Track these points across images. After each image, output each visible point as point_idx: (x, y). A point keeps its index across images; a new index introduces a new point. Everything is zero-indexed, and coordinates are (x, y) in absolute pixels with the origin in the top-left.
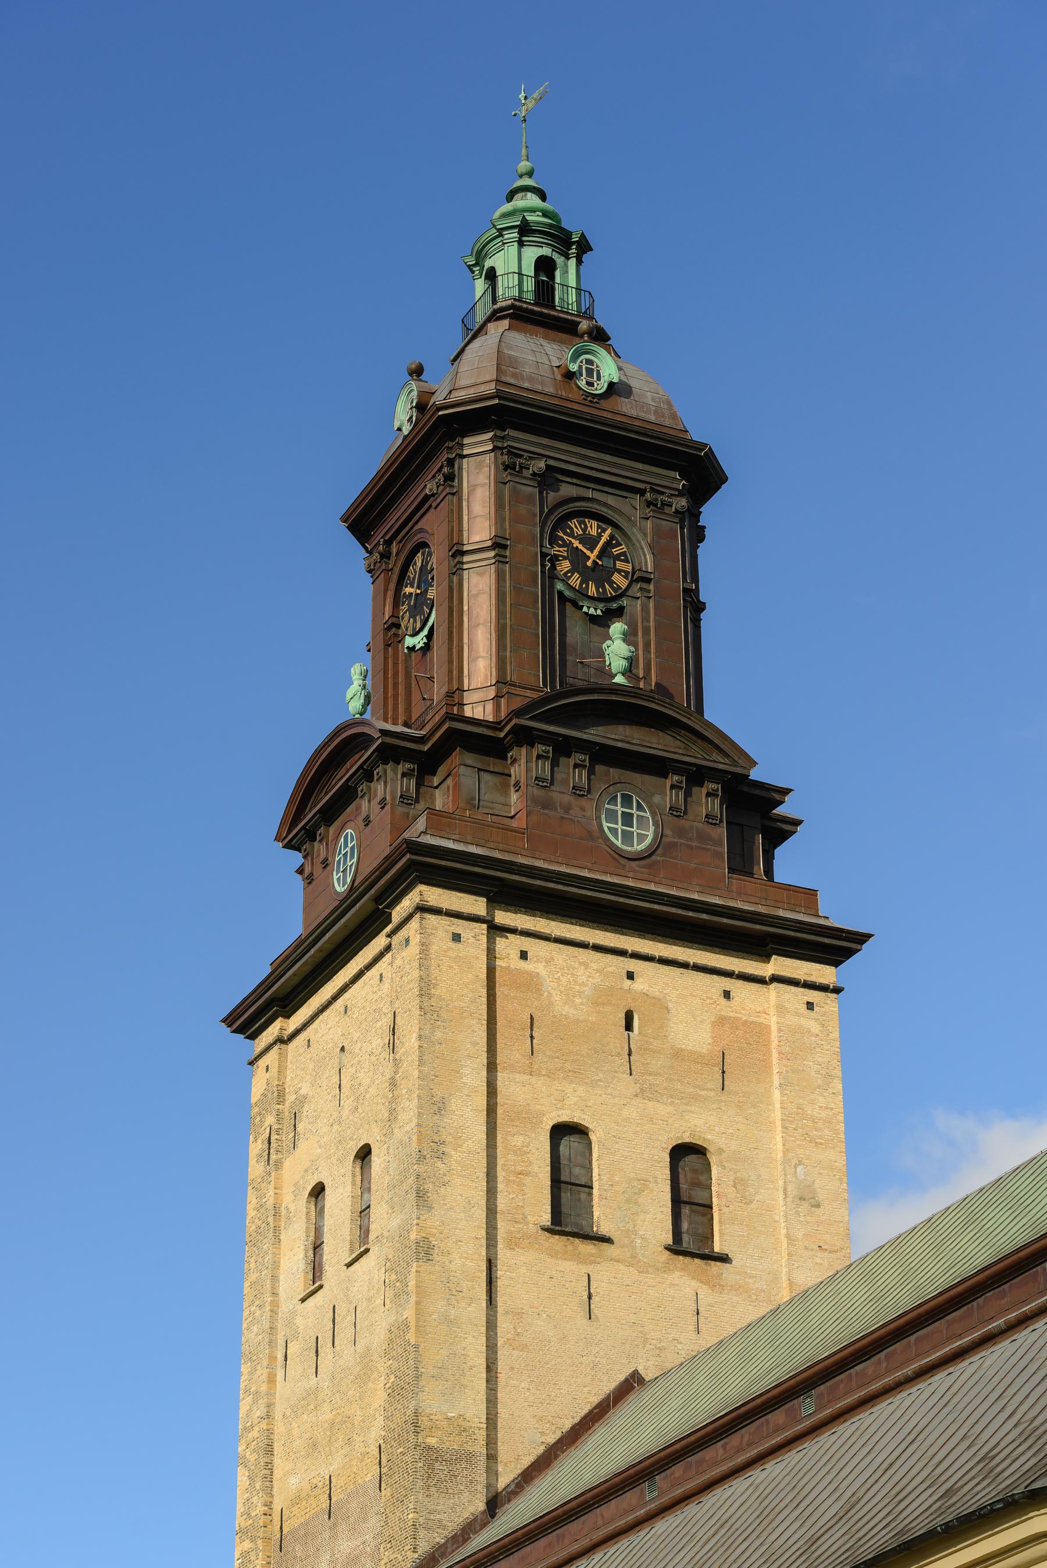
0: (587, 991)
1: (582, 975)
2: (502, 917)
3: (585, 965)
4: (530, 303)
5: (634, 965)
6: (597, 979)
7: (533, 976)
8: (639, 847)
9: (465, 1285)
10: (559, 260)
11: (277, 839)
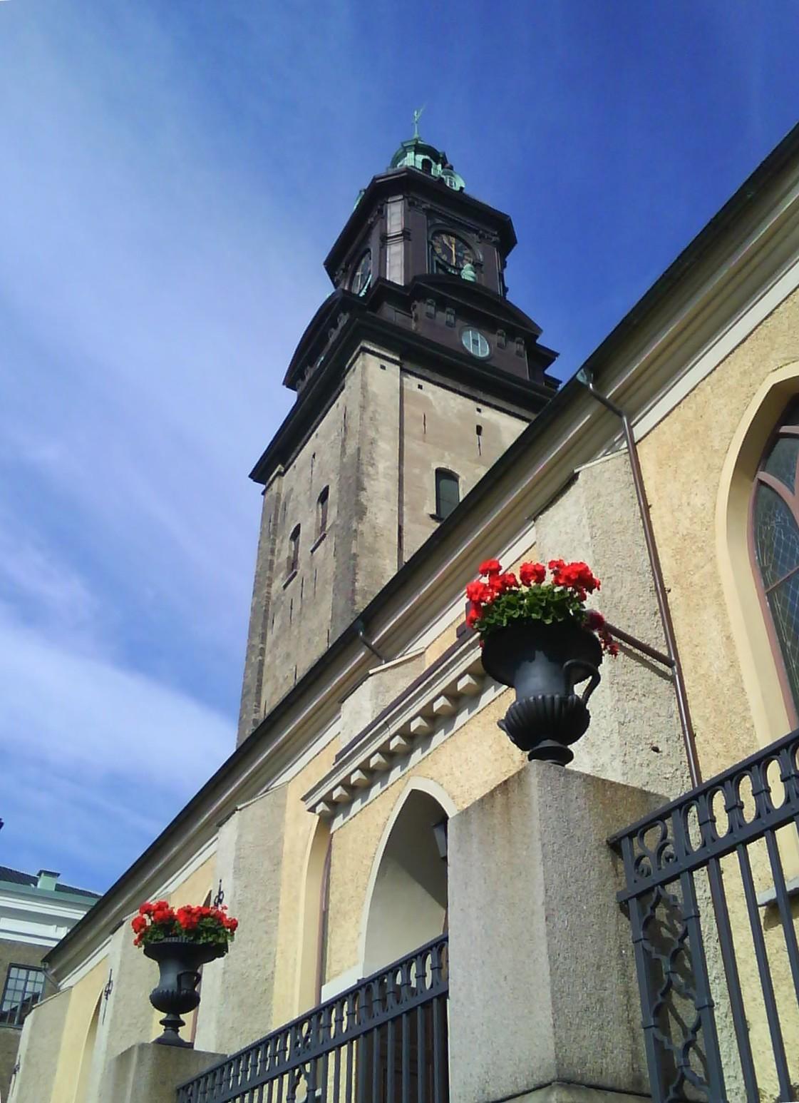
0: (455, 411)
1: (452, 403)
2: (407, 366)
3: (455, 400)
4: (419, 169)
5: (480, 406)
7: (426, 398)
8: (480, 355)
9: (386, 533)
10: (434, 163)
11: (284, 384)
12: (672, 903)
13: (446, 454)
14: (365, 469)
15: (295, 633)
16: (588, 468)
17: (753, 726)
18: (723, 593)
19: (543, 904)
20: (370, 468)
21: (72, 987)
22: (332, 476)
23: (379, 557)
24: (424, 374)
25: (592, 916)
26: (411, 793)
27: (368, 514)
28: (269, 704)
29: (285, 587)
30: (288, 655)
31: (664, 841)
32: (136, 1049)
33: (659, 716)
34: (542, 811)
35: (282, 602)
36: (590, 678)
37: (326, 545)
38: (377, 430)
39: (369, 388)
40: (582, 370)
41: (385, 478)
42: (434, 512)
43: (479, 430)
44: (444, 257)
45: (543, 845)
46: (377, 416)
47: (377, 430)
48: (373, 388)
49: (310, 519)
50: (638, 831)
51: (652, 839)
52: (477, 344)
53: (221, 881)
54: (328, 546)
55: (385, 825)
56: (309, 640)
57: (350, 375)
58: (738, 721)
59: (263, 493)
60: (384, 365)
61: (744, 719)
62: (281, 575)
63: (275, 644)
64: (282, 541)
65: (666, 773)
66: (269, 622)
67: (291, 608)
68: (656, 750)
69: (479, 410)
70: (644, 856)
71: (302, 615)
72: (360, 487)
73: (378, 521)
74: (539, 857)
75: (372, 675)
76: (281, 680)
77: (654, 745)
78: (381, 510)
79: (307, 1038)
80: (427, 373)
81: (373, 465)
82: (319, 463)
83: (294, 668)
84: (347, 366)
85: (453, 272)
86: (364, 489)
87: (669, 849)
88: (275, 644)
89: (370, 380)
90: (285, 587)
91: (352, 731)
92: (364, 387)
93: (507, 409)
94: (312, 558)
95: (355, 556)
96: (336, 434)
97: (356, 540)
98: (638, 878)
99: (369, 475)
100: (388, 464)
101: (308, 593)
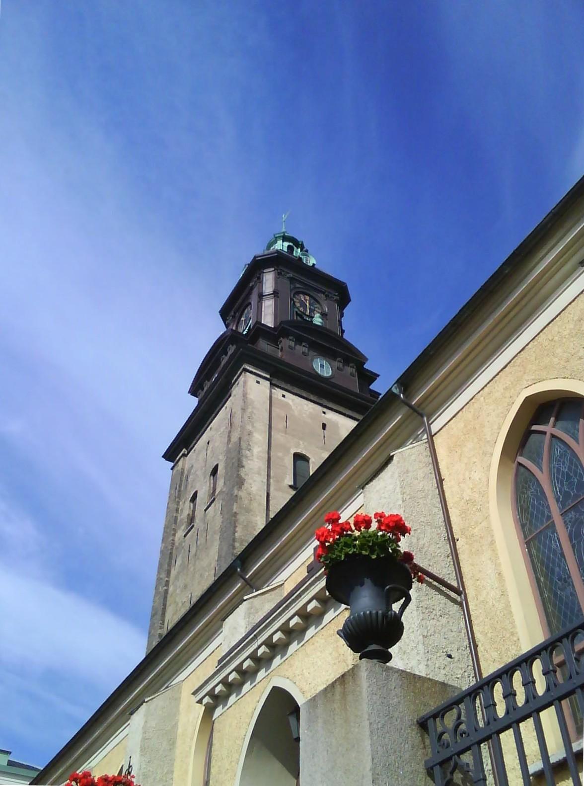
0: (308, 413)
1: (306, 408)
2: (275, 381)
3: (307, 405)
4: (285, 251)
5: (325, 410)
6: (311, 410)
8: (325, 375)
9: (258, 497)
10: (295, 248)
11: (189, 393)
12: (466, 769)
13: (301, 443)
14: (244, 453)
15: (192, 569)
16: (400, 452)
17: (519, 639)
18: (495, 542)
19: (371, 769)
20: (248, 452)
22: (221, 457)
23: (252, 515)
24: (286, 387)
25: (407, 779)
26: (272, 688)
28: (171, 623)
29: (185, 536)
30: (185, 586)
31: (459, 721)
33: (452, 632)
34: (369, 698)
35: (183, 547)
36: (404, 599)
37: (215, 506)
38: (253, 426)
39: (248, 396)
40: (396, 385)
41: (258, 459)
42: (292, 483)
43: (324, 426)
44: (301, 309)
45: (371, 724)
46: (253, 416)
47: (253, 425)
48: (251, 396)
49: (204, 487)
50: (439, 714)
51: (450, 719)
52: (323, 368)
53: (130, 757)
54: (217, 506)
55: (253, 713)
56: (201, 575)
57: (235, 388)
58: (508, 635)
59: (172, 469)
60: (260, 381)
61: (512, 634)
62: (183, 527)
63: (177, 578)
66: (173, 562)
67: (189, 552)
68: (450, 656)
69: (324, 413)
70: (444, 733)
71: (197, 557)
72: (240, 465)
73: (252, 489)
74: (368, 733)
76: (180, 605)
77: (449, 653)
78: (255, 481)
80: (288, 387)
81: (249, 450)
82: (212, 448)
84: (233, 382)
85: (307, 319)
86: (243, 467)
87: (463, 727)
88: (177, 578)
89: (249, 391)
90: (185, 536)
91: (230, 642)
92: (245, 395)
93: (344, 412)
96: (224, 428)
97: (237, 503)
98: (440, 749)
99: (246, 457)
100: (260, 449)
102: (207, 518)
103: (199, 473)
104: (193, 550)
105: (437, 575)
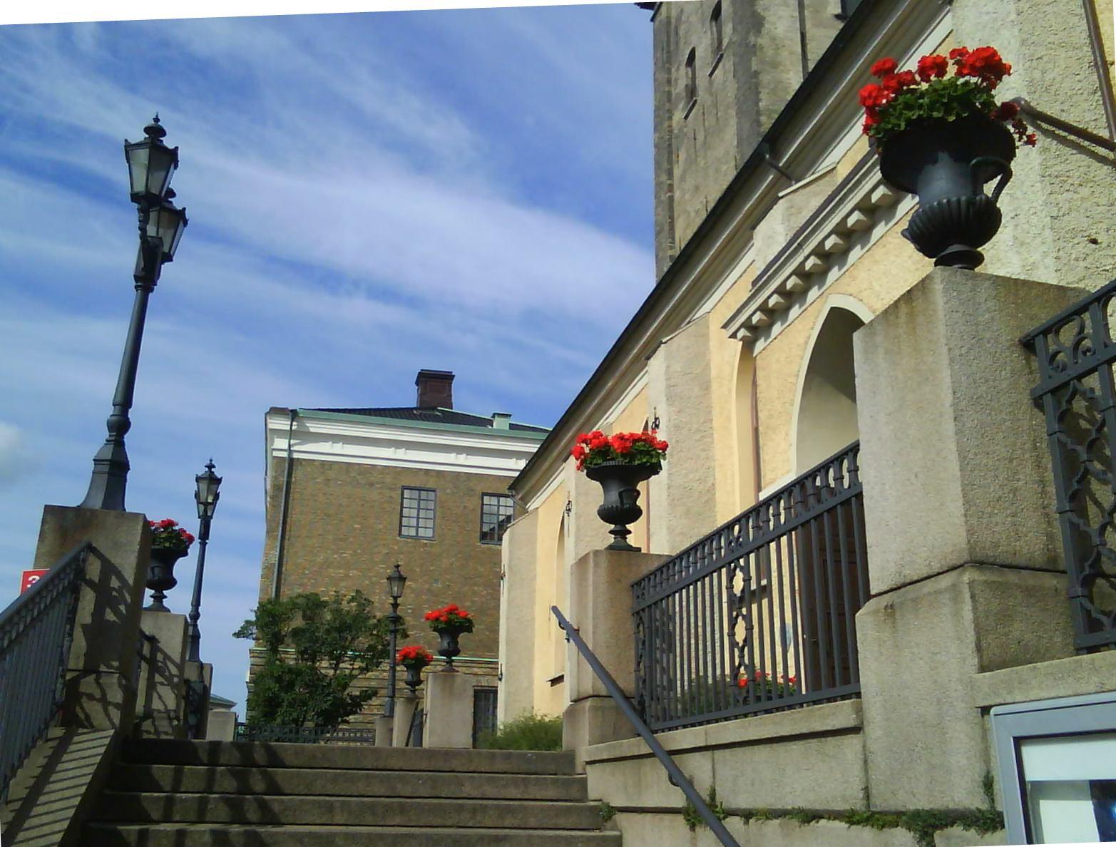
9: (787, 42)
12: (1089, 395)
15: (702, 163)
19: (951, 406)
21: (537, 508)
25: (1004, 413)
27: (766, 26)
29: (686, 117)
30: (697, 188)
31: (1082, 335)
32: (591, 555)
34: (947, 317)
35: (685, 135)
36: (999, 177)
37: (724, 66)
42: (839, 11)
45: (950, 349)
50: (1053, 328)
51: (1067, 335)
53: (655, 409)
54: (727, 67)
55: (806, 343)
56: (717, 170)
59: (653, 20)
62: (681, 106)
63: (683, 179)
64: (678, 69)
65: (1105, 266)
66: (674, 157)
67: (695, 139)
68: (1094, 242)
70: (1060, 352)
74: (946, 361)
75: (782, 197)
76: (693, 214)
78: (780, 18)
79: (739, 537)
83: (705, 200)
87: (1087, 343)
88: (683, 179)
90: (686, 117)
94: (711, 83)
95: (756, 74)
98: (1052, 373)
101: (711, 121)
102: (715, 86)
103: (694, 19)
104: (700, 137)
105: (1075, 124)
